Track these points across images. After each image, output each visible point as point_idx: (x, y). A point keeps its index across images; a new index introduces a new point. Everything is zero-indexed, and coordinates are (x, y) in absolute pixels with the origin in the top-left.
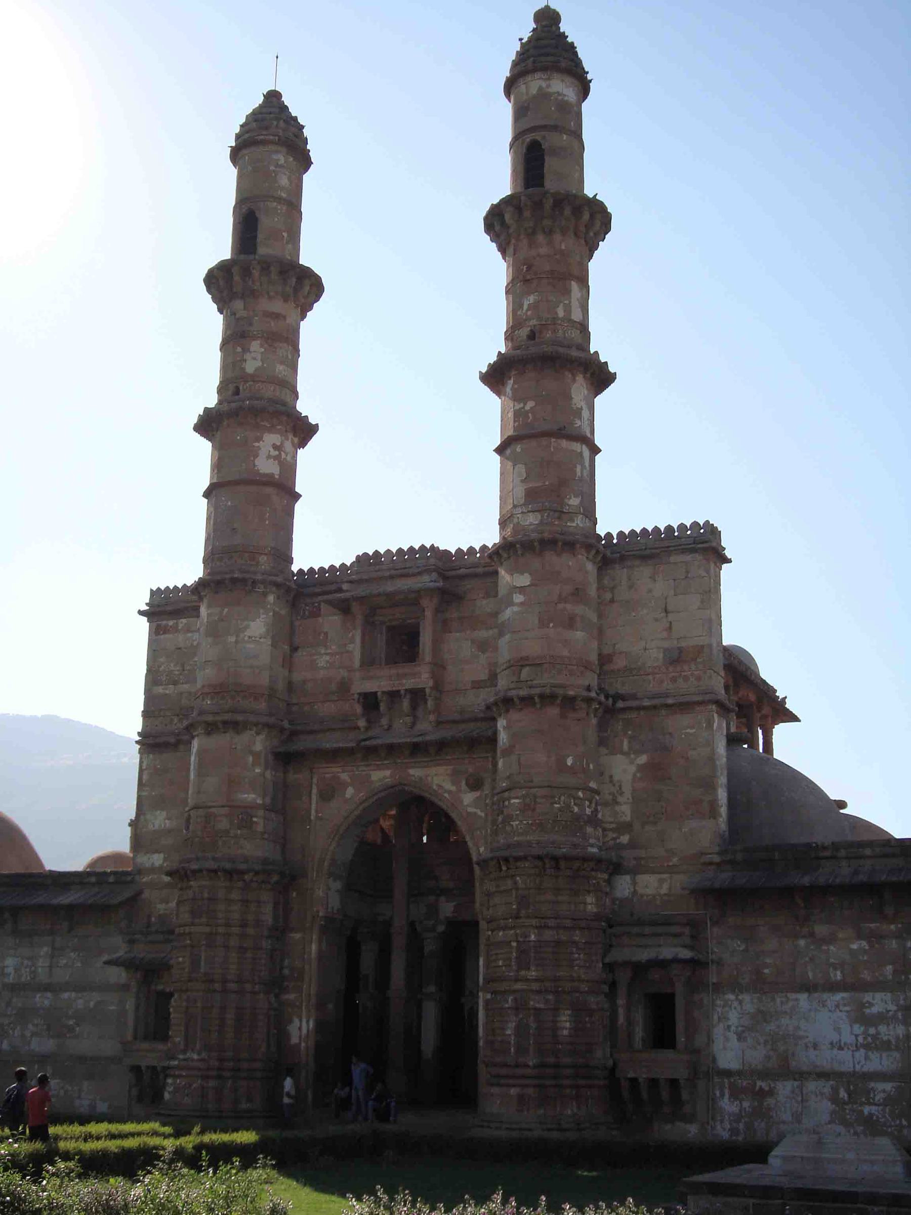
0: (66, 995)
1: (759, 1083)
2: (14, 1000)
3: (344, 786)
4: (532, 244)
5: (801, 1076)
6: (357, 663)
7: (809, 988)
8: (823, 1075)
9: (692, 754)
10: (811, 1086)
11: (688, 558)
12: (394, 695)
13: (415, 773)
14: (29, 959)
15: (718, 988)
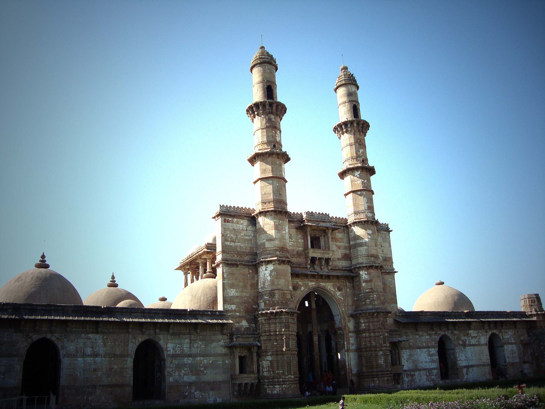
0: (199, 358)
1: (412, 373)
2: (174, 361)
3: (301, 286)
4: (360, 135)
5: (420, 370)
6: (310, 247)
7: (419, 348)
8: (424, 369)
9: (391, 286)
10: (422, 372)
11: (385, 233)
12: (320, 259)
13: (322, 284)
14: (179, 344)
15: (402, 349)
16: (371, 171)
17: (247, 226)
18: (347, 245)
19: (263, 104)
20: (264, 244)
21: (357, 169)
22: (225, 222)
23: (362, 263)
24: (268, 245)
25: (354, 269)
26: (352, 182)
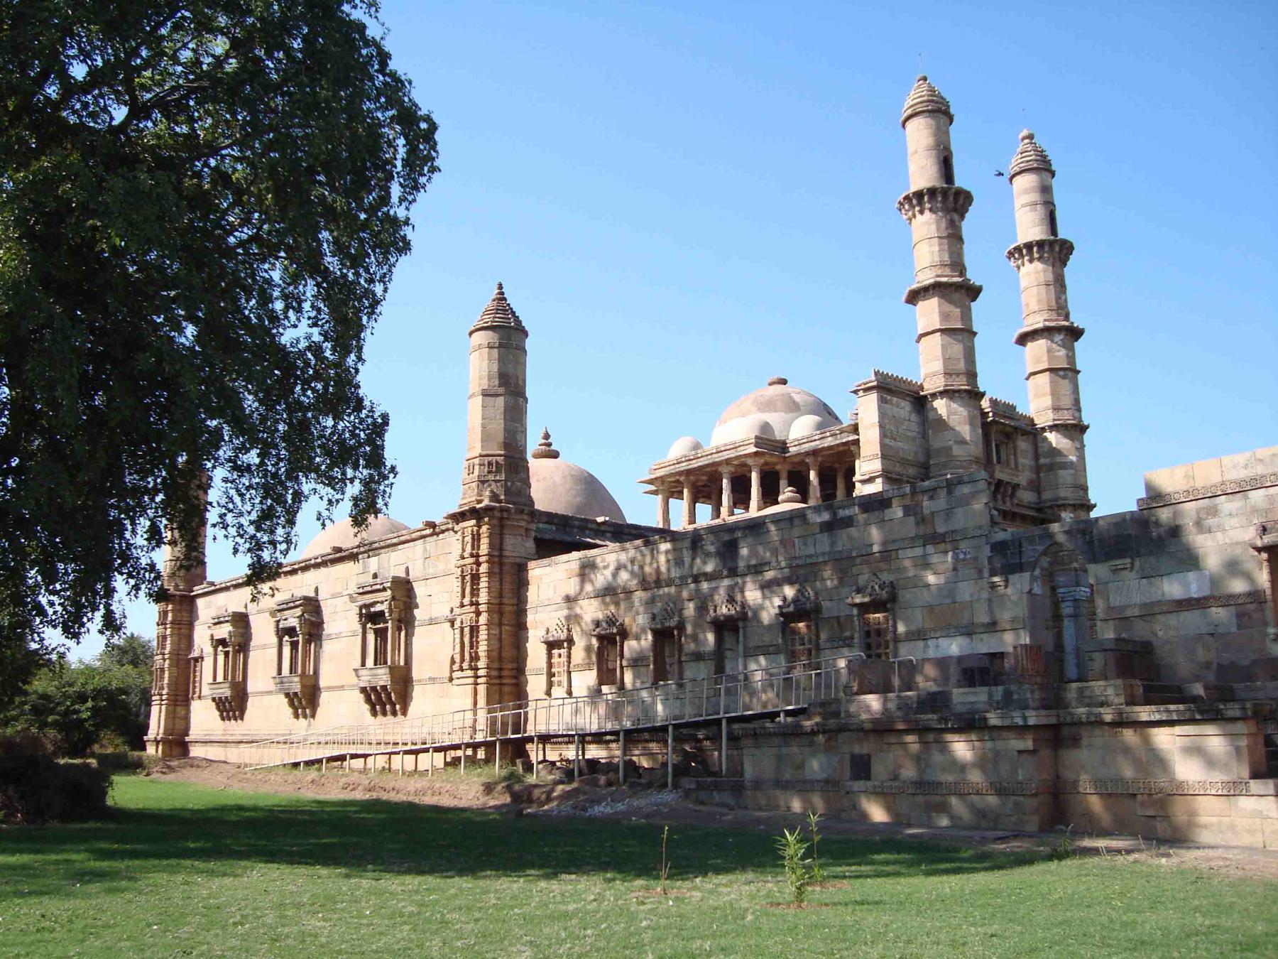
16: (1075, 333)
17: (910, 413)
18: (1032, 463)
19: (932, 192)
20: (950, 449)
21: (1058, 329)
22: (882, 401)
23: (1065, 499)
24: (957, 451)
25: (1051, 507)
26: (1049, 351)
